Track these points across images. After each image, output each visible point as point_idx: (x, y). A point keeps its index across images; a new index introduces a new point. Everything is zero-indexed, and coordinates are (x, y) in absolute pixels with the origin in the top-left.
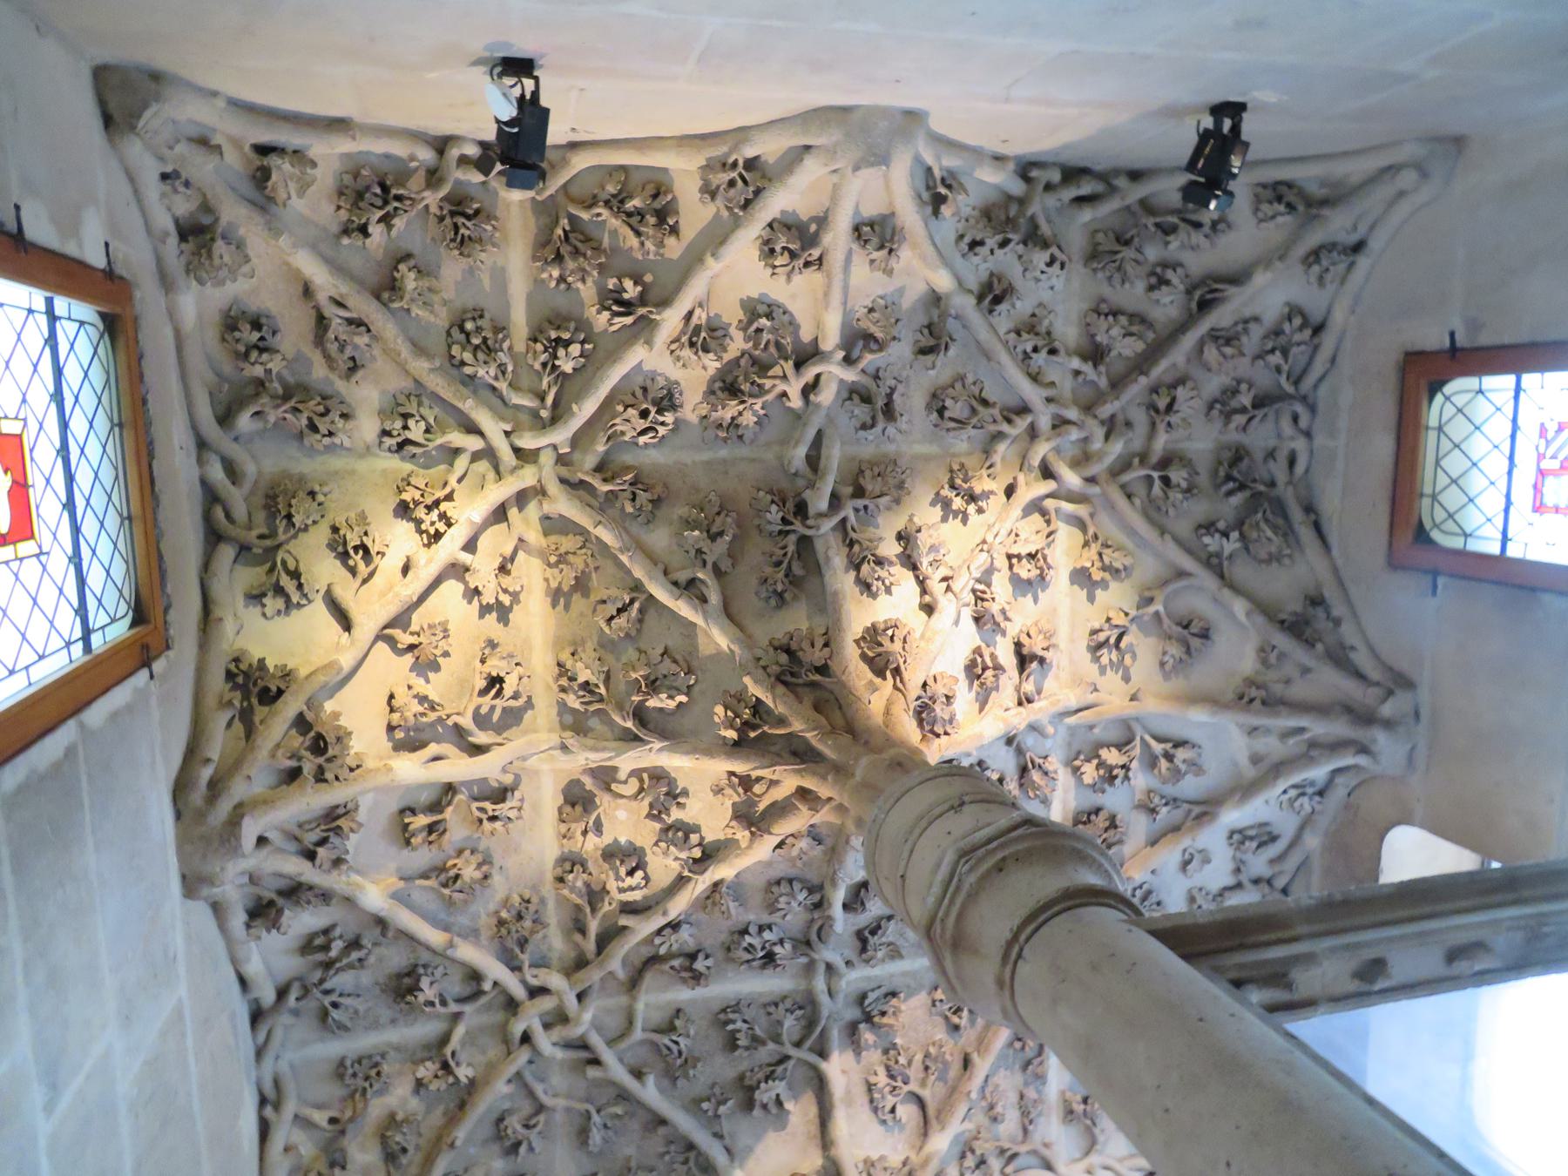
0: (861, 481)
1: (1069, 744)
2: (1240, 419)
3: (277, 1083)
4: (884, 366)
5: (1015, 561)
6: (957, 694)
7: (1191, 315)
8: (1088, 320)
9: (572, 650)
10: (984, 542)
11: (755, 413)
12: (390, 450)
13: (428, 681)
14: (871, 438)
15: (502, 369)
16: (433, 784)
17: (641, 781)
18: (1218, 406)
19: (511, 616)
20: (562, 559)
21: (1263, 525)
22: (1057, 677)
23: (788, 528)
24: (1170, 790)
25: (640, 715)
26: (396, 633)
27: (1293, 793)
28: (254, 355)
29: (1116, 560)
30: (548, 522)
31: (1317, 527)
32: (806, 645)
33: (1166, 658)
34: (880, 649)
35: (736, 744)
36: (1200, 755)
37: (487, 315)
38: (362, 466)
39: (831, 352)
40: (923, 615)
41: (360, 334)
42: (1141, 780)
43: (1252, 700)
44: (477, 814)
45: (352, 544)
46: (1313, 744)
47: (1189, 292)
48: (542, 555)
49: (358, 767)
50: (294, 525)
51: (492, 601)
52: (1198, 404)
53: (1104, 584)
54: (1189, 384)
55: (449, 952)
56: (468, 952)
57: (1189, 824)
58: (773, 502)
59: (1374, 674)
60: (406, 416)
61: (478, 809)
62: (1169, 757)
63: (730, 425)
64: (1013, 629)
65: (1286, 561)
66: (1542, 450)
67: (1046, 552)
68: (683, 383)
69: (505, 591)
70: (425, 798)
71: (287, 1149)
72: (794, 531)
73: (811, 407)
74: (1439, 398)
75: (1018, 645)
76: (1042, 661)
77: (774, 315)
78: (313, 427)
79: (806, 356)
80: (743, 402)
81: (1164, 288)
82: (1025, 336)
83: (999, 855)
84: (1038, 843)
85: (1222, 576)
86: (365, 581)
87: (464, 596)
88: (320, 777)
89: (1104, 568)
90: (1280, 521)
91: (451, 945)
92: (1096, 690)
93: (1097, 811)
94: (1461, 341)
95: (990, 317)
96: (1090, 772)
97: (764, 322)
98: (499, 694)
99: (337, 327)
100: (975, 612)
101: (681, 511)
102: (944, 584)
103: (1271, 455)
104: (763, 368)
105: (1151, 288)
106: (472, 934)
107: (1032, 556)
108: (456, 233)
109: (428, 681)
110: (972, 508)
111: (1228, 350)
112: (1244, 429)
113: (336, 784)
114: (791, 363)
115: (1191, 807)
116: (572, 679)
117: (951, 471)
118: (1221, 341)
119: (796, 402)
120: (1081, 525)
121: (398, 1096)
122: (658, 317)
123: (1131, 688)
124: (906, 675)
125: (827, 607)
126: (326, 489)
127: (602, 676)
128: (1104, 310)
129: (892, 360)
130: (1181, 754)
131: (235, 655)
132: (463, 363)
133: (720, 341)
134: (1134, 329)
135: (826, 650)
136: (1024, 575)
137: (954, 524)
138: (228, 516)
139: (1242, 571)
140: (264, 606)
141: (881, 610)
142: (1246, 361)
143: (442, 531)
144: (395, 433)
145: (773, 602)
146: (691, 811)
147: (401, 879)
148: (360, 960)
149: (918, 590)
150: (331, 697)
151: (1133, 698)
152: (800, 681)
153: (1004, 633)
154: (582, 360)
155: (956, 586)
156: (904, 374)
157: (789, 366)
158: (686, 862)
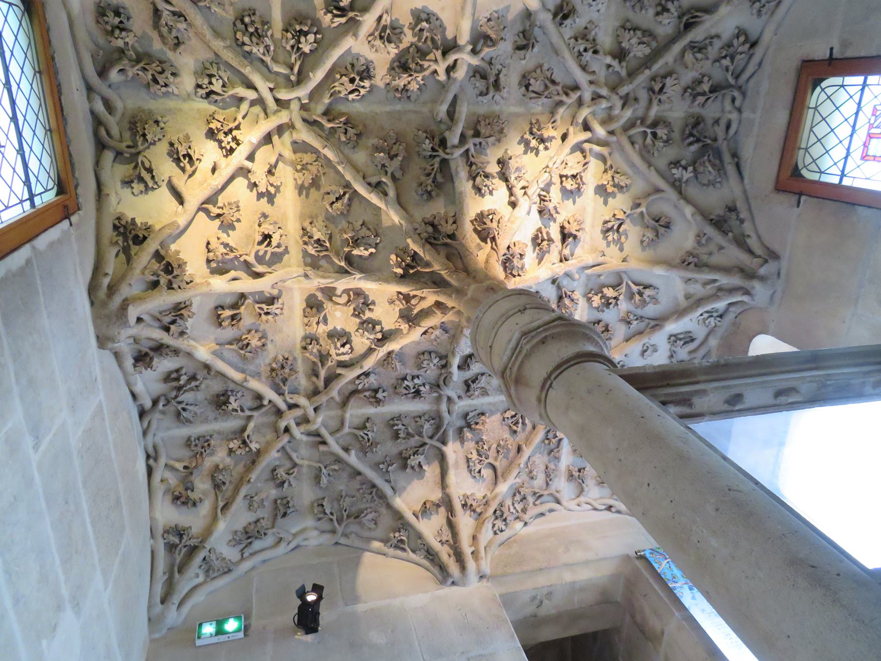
0: (479, 128)
1: (587, 285)
2: (701, 99)
3: (155, 448)
4: (495, 57)
5: (564, 179)
6: (527, 254)
7: (679, 32)
8: (618, 33)
9: (310, 221)
10: (547, 167)
11: (418, 83)
12: (202, 97)
13: (228, 236)
14: (485, 101)
15: (267, 48)
16: (233, 293)
17: (349, 296)
18: (689, 90)
19: (275, 200)
20: (304, 167)
21: (707, 164)
22: (583, 247)
23: (435, 154)
24: (639, 312)
25: (349, 259)
26: (210, 207)
27: (706, 315)
28: (117, 32)
29: (622, 180)
30: (296, 145)
31: (738, 166)
32: (443, 222)
33: (645, 239)
34: (485, 226)
35: (402, 276)
36: (657, 293)
37: (257, 12)
38: (186, 106)
39: (464, 46)
40: (510, 208)
41: (180, 22)
42: (624, 305)
43: (689, 264)
44: (258, 310)
45: (182, 153)
46: (720, 289)
47: (680, 17)
48: (293, 164)
49: (191, 281)
50: (147, 141)
51: (264, 191)
52: (678, 88)
53: (613, 195)
54: (674, 76)
55: (245, 384)
56: (255, 384)
57: (648, 330)
58: (427, 137)
59: (758, 251)
60: (210, 76)
61: (259, 308)
62: (641, 294)
63: (403, 89)
64: (560, 219)
65: (718, 185)
66: (872, 122)
67: (582, 174)
68: (376, 63)
69: (272, 185)
70: (229, 301)
71: (162, 481)
72: (438, 156)
73: (451, 81)
74: (818, 89)
75: (562, 228)
76: (575, 237)
77: (431, 20)
78: (156, 81)
79: (449, 47)
80: (411, 75)
81: (665, 14)
82: (580, 41)
83: (543, 335)
84: (564, 329)
85: (680, 193)
86: (190, 176)
87: (248, 187)
88: (170, 286)
89: (614, 186)
90: (717, 162)
91: (246, 380)
92: (604, 255)
93: (599, 322)
94: (836, 54)
95: (560, 28)
96: (597, 300)
97: (424, 24)
98: (269, 244)
99: (166, 17)
100: (539, 207)
101: (373, 141)
102: (523, 191)
103: (717, 122)
104: (423, 54)
105: (658, 14)
106: (257, 375)
107: (574, 177)
109: (228, 236)
110: (541, 147)
111: (699, 56)
112: (703, 105)
113: (179, 290)
114: (440, 52)
115: (650, 321)
116: (311, 237)
117: (531, 124)
118: (696, 50)
119: (442, 77)
120: (604, 160)
121: (220, 456)
122: (360, 19)
123: (624, 254)
124: (498, 241)
125: (456, 201)
126: (165, 119)
127: (328, 236)
128: (628, 27)
129: (500, 52)
130: (647, 292)
131: (119, 215)
132: (244, 44)
133: (398, 36)
134: (645, 39)
135: (454, 225)
136: (569, 187)
137: (531, 155)
138: (108, 133)
139: (692, 191)
140: (132, 188)
141: (486, 204)
142: (709, 62)
143: (234, 147)
144: (204, 86)
145: (425, 197)
146: (376, 313)
147: (217, 344)
148: (197, 386)
149: (508, 193)
150: (174, 242)
151: (624, 260)
152: (439, 243)
153: (555, 221)
154: (315, 45)
155: (530, 191)
156: (507, 62)
157: (439, 54)
158: (373, 340)
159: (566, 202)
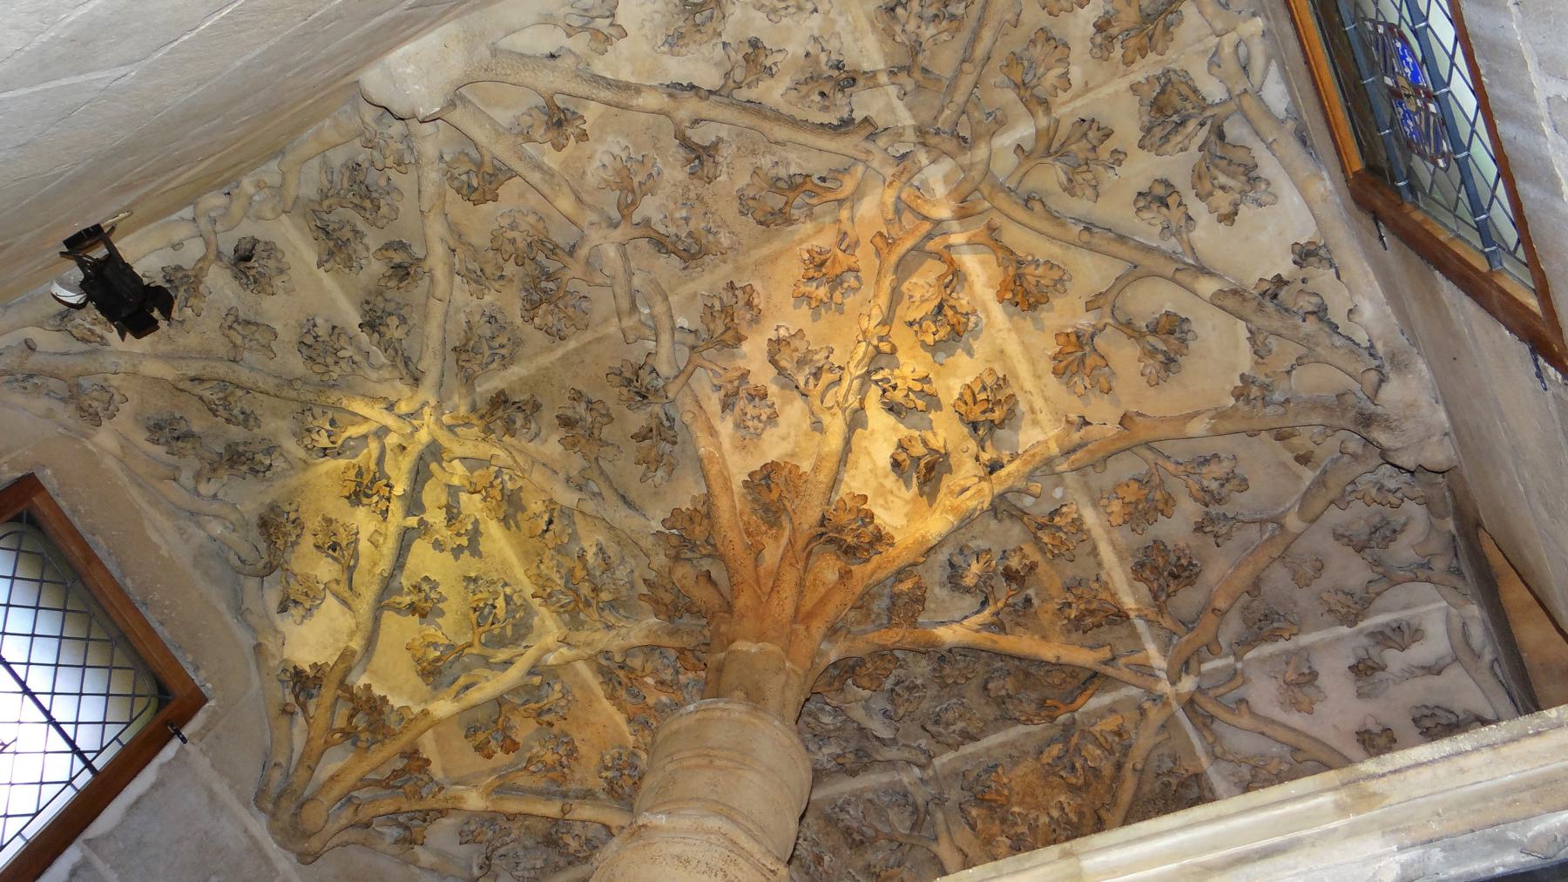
19: (481, 548)
38: (310, 475)
67: (952, 302)
106: (587, 795)
108: (247, 277)
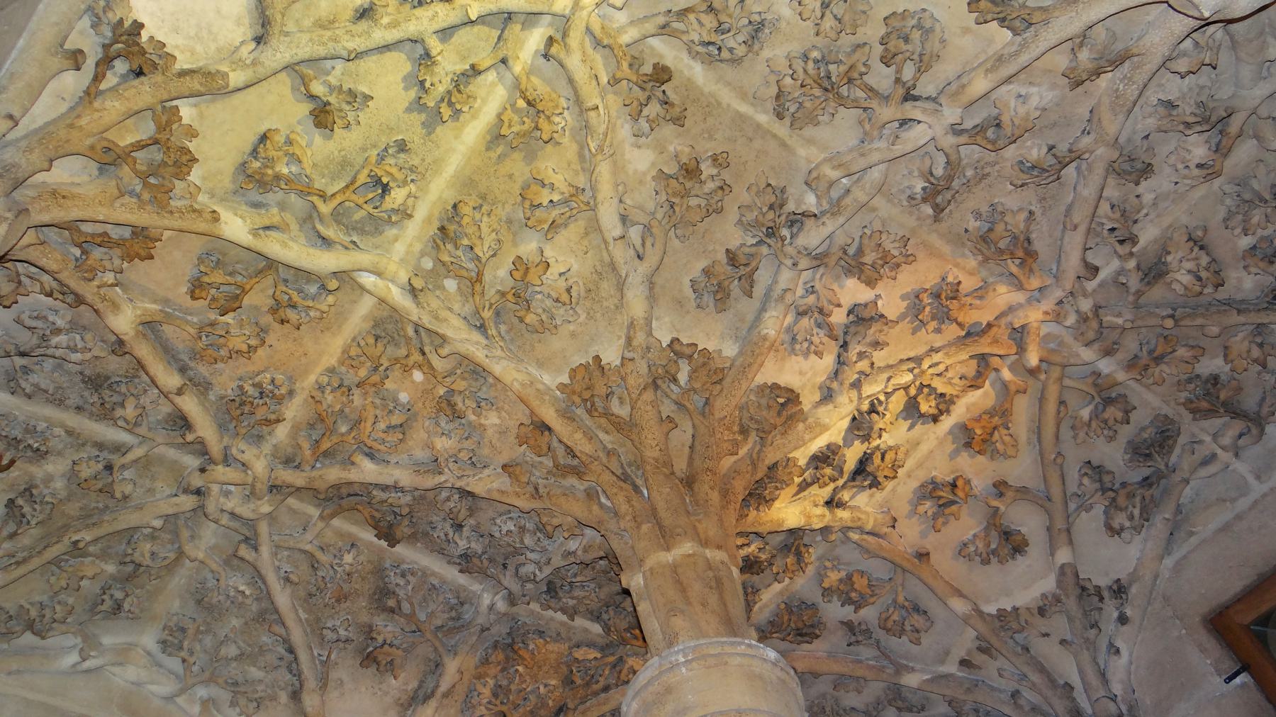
48: (518, 88)
51: (431, 104)
87: (405, 79)
91: (180, 392)
159: (901, 421)
